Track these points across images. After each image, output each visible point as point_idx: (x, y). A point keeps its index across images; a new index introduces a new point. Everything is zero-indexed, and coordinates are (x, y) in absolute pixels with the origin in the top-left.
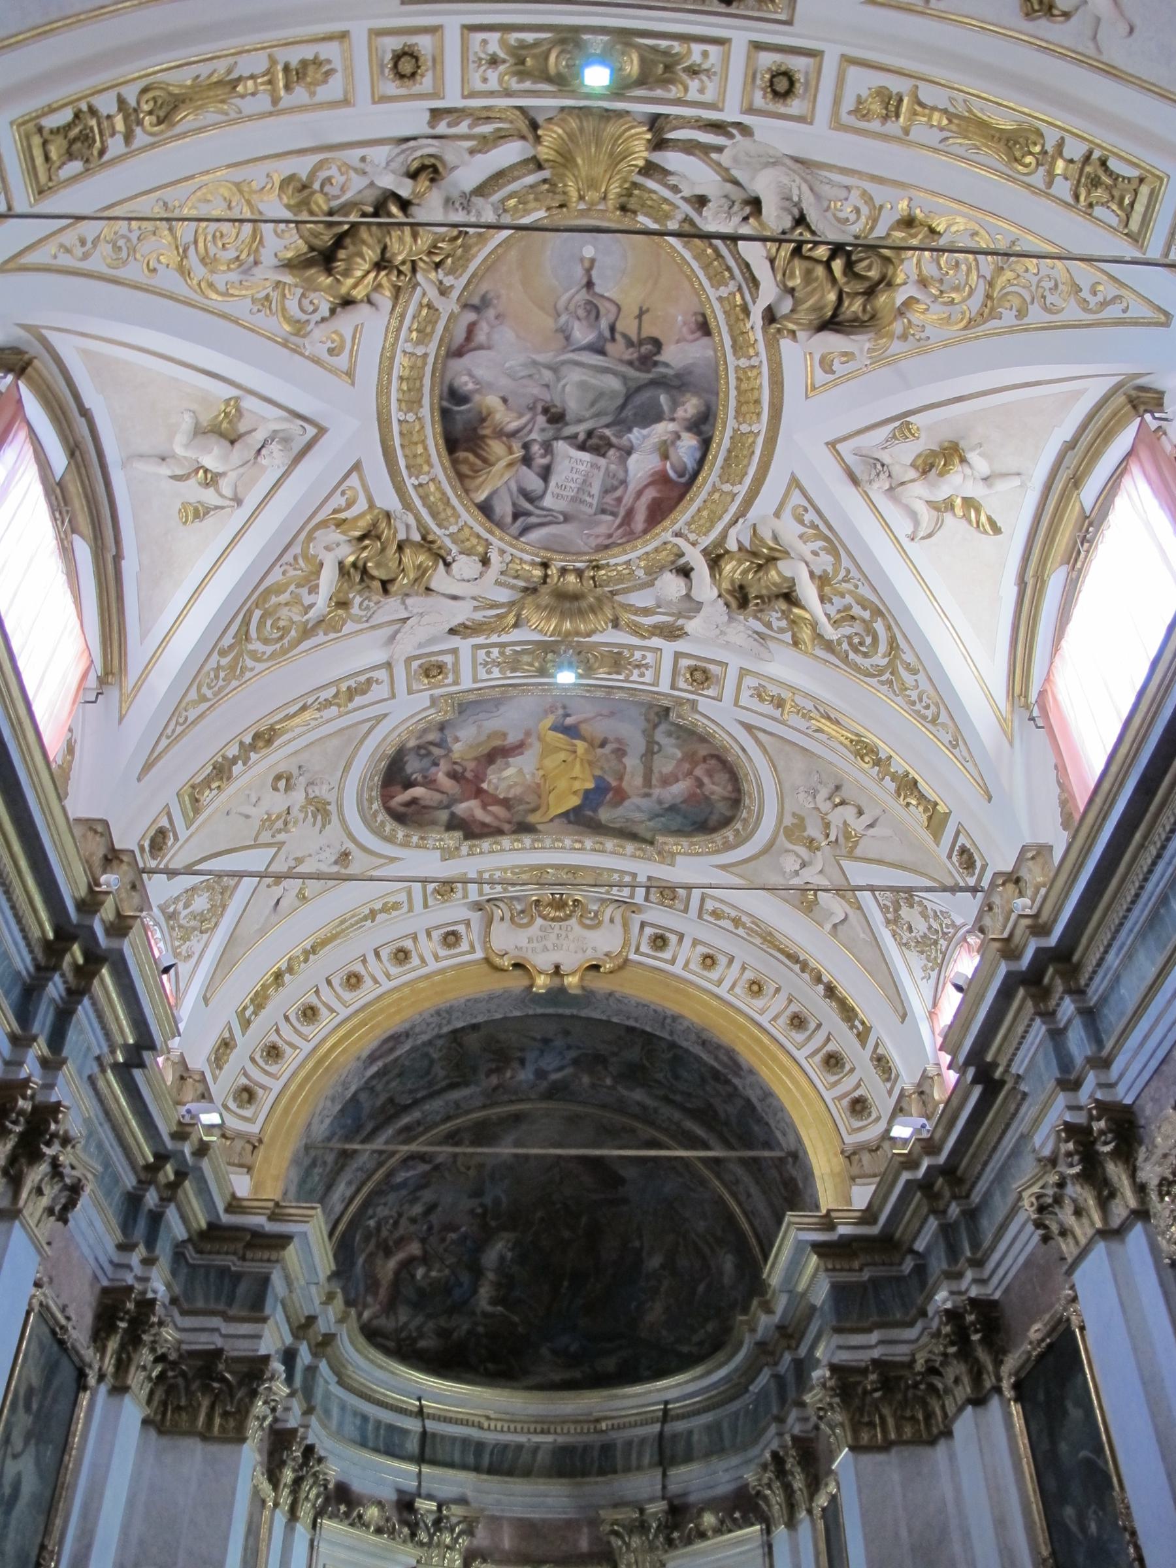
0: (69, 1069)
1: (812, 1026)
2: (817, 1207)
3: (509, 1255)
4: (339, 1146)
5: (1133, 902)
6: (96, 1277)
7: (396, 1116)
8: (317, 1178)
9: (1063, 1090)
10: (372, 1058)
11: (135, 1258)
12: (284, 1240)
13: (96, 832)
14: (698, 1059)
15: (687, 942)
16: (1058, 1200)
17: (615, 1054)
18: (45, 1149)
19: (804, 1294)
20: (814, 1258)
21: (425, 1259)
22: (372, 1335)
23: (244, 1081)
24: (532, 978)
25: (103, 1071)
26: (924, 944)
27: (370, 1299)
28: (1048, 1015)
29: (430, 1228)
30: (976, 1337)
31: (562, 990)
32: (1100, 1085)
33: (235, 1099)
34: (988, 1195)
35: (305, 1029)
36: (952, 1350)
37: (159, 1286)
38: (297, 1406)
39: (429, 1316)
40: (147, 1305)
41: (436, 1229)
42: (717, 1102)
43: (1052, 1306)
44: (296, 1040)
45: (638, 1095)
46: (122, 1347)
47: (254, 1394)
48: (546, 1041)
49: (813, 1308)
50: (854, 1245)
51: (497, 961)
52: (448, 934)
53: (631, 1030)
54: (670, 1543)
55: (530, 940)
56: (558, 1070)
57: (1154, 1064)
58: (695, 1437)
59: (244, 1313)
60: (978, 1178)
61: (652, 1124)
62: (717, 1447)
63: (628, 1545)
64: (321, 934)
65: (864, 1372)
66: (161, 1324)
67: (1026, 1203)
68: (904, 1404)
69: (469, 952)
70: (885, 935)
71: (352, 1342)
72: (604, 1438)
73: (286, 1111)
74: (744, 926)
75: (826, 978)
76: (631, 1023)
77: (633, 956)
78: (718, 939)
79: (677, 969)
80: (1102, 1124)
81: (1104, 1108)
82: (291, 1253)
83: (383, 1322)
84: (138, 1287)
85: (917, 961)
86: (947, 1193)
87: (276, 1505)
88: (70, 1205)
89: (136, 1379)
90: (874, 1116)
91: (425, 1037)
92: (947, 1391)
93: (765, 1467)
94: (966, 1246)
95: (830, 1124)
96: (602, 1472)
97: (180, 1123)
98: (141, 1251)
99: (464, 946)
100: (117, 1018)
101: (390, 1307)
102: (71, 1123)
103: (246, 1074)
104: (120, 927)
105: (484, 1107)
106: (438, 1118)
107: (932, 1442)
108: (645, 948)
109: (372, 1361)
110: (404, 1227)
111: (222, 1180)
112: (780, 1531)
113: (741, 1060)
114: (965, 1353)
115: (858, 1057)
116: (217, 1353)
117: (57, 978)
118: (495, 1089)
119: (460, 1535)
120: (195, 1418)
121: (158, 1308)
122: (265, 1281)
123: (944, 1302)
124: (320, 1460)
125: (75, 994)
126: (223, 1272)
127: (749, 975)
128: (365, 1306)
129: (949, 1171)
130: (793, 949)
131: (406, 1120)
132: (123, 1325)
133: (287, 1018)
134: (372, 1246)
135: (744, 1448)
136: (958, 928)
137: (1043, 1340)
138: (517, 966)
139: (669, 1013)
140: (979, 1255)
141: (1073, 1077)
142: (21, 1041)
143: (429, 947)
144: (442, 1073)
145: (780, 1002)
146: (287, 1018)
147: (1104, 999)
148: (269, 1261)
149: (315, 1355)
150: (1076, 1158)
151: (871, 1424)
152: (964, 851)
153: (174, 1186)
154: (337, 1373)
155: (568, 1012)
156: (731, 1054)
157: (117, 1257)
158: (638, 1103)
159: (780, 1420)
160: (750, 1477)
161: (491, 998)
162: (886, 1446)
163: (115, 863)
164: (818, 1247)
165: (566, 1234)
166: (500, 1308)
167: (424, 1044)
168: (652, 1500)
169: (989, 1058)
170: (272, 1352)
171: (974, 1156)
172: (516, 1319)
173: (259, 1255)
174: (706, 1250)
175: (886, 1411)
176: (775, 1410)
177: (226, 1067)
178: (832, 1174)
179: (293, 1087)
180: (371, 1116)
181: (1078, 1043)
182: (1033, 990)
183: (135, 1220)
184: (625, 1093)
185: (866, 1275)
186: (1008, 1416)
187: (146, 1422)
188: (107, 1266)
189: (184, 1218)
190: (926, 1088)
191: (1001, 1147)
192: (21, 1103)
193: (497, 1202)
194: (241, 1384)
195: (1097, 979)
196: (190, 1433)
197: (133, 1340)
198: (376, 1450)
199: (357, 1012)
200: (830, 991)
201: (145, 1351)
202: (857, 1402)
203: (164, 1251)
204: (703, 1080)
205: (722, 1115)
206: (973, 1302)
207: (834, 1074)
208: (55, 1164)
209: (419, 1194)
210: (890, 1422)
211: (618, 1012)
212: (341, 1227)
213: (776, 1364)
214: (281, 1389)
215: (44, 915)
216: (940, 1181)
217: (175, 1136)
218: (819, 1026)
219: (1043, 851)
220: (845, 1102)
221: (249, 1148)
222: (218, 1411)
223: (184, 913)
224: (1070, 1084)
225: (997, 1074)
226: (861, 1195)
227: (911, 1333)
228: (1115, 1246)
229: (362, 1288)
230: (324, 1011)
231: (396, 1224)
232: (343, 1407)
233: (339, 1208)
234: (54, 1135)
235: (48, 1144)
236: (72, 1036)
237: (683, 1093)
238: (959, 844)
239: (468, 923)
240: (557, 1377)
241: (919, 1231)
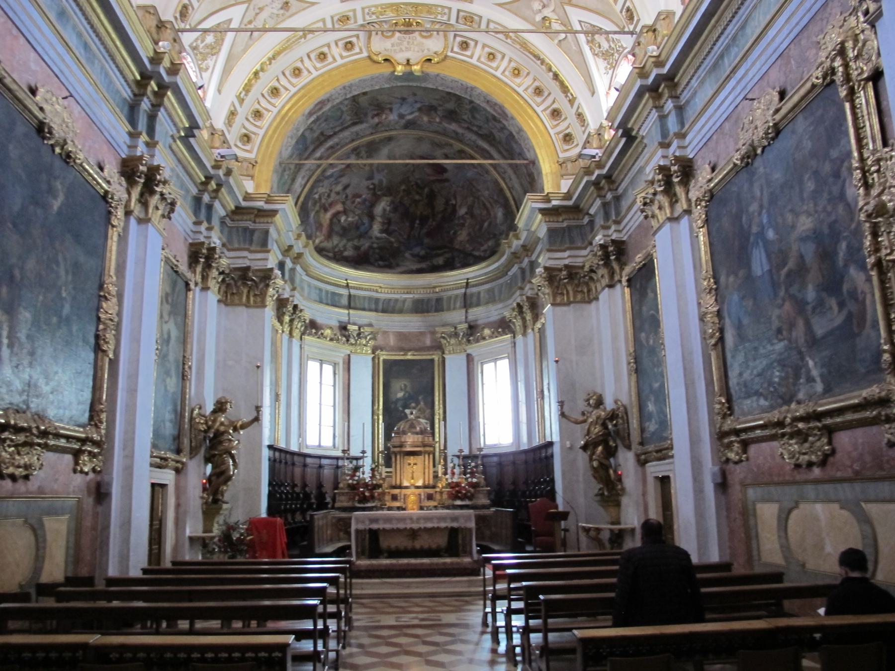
0: (160, 147)
1: (546, 94)
2: (542, 190)
3: (388, 208)
4: (297, 162)
5: (707, 55)
6: (186, 239)
7: (325, 140)
8: (286, 177)
9: (662, 147)
10: (311, 114)
11: (203, 228)
12: (274, 212)
13: (150, 13)
14: (485, 110)
15: (479, 46)
16: (652, 201)
17: (440, 106)
18: (157, 189)
19: (534, 232)
20: (540, 216)
21: (345, 212)
22: (320, 251)
23: (244, 131)
24: (394, 67)
25: (175, 141)
26: (606, 55)
27: (318, 234)
28: (659, 108)
29: (347, 197)
30: (613, 258)
31: (411, 73)
32: (679, 147)
34: (626, 190)
35: (273, 101)
36: (601, 263)
37: (216, 240)
38: (288, 288)
39: (348, 240)
40: (212, 250)
41: (350, 197)
42: (495, 131)
43: (648, 246)
44: (270, 107)
45: (453, 127)
46: (203, 270)
47: (267, 286)
48: (404, 99)
49: (539, 238)
50: (560, 210)
51: (375, 58)
52: (347, 43)
53: (449, 93)
54: (469, 341)
55: (393, 45)
56: (409, 112)
57: (705, 140)
58: (482, 295)
59: (259, 249)
60: (622, 181)
61: (461, 141)
62: (492, 298)
63: (449, 342)
64: (277, 48)
65: (560, 270)
66: (220, 257)
67: (638, 200)
68: (578, 285)
69: (360, 53)
70: (586, 49)
71: (312, 256)
73: (268, 146)
74: (511, 38)
75: (554, 69)
76: (449, 90)
77: (450, 54)
78: (496, 44)
79: (474, 61)
80: (676, 168)
81: (678, 160)
82: (278, 218)
84: (207, 242)
85: (602, 64)
86: (606, 187)
87: (283, 332)
88: (172, 210)
89: (213, 284)
90: (575, 143)
91: (338, 101)
92: (598, 280)
93: (513, 309)
94: (613, 213)
95: (552, 147)
96: (437, 311)
97: (216, 161)
98: (205, 225)
99: (357, 50)
100: (178, 115)
101: (329, 236)
102: (165, 174)
103: (244, 127)
104: (175, 69)
105: (372, 134)
107: (590, 302)
108: (456, 49)
109: (322, 264)
111: (240, 186)
112: (519, 337)
113: (507, 111)
114: (607, 264)
115: (569, 112)
116: (248, 269)
117: (145, 99)
118: (377, 125)
119: (370, 339)
120: (241, 298)
121: (218, 251)
122: (267, 232)
123: (600, 240)
124: (301, 311)
125: (156, 106)
126: (246, 229)
127: (513, 65)
128: (316, 237)
129: (608, 177)
130: (537, 52)
131: (330, 143)
132: (202, 260)
133: (263, 95)
134: (317, 208)
136: (625, 49)
138: (386, 60)
139: (469, 85)
140: (619, 219)
141: (667, 141)
142: (134, 135)
143: (336, 51)
144: (348, 118)
145: (528, 81)
146: (263, 95)
147: (688, 102)
149: (294, 263)
150: (662, 183)
151: (562, 294)
152: (628, 10)
153: (217, 191)
154: (305, 271)
155: (415, 84)
156: (501, 108)
157: (195, 228)
158: (454, 131)
159: (522, 289)
160: (507, 314)
161: (372, 79)
162: (569, 303)
163: (163, 29)
164: (543, 211)
165: (417, 197)
166: (384, 235)
167: (338, 104)
168: (460, 323)
169: (629, 126)
170: (274, 266)
171: (621, 171)
172: (393, 240)
173: (262, 220)
174: (488, 205)
175: (570, 288)
176: (520, 284)
177: (234, 125)
178: (552, 173)
179: (270, 132)
180: (312, 143)
181: (672, 124)
182: (653, 94)
183: (200, 209)
184: (446, 125)
185: (565, 224)
186: (623, 294)
187: (219, 301)
188: (191, 234)
189: (223, 206)
190: (602, 132)
191: (632, 170)
192: (141, 168)
193: (381, 181)
194: (261, 281)
195: (685, 92)
196: (239, 305)
197: (208, 266)
198: (327, 304)
200: (556, 76)
201: (214, 271)
202: (556, 284)
203: (216, 222)
204: (488, 120)
205: (497, 137)
206: (613, 241)
208: (162, 194)
209: (340, 180)
210: (571, 293)
211: (442, 85)
212: (301, 199)
213: (521, 263)
214: (280, 282)
215: (133, 68)
216: (603, 182)
217: (214, 167)
218: (550, 94)
219: (669, 15)
220: (561, 136)
221: (251, 166)
222: (252, 294)
223: (201, 46)
224: (665, 145)
225: (634, 133)
226: (565, 185)
227: (584, 252)
228: (675, 225)
229: (314, 230)
230: (282, 90)
232: (309, 285)
233: (299, 190)
234: (159, 181)
235: (157, 185)
236: (158, 128)
237: (477, 126)
238: (626, 6)
239: (358, 37)
240: (415, 266)
241: (592, 205)
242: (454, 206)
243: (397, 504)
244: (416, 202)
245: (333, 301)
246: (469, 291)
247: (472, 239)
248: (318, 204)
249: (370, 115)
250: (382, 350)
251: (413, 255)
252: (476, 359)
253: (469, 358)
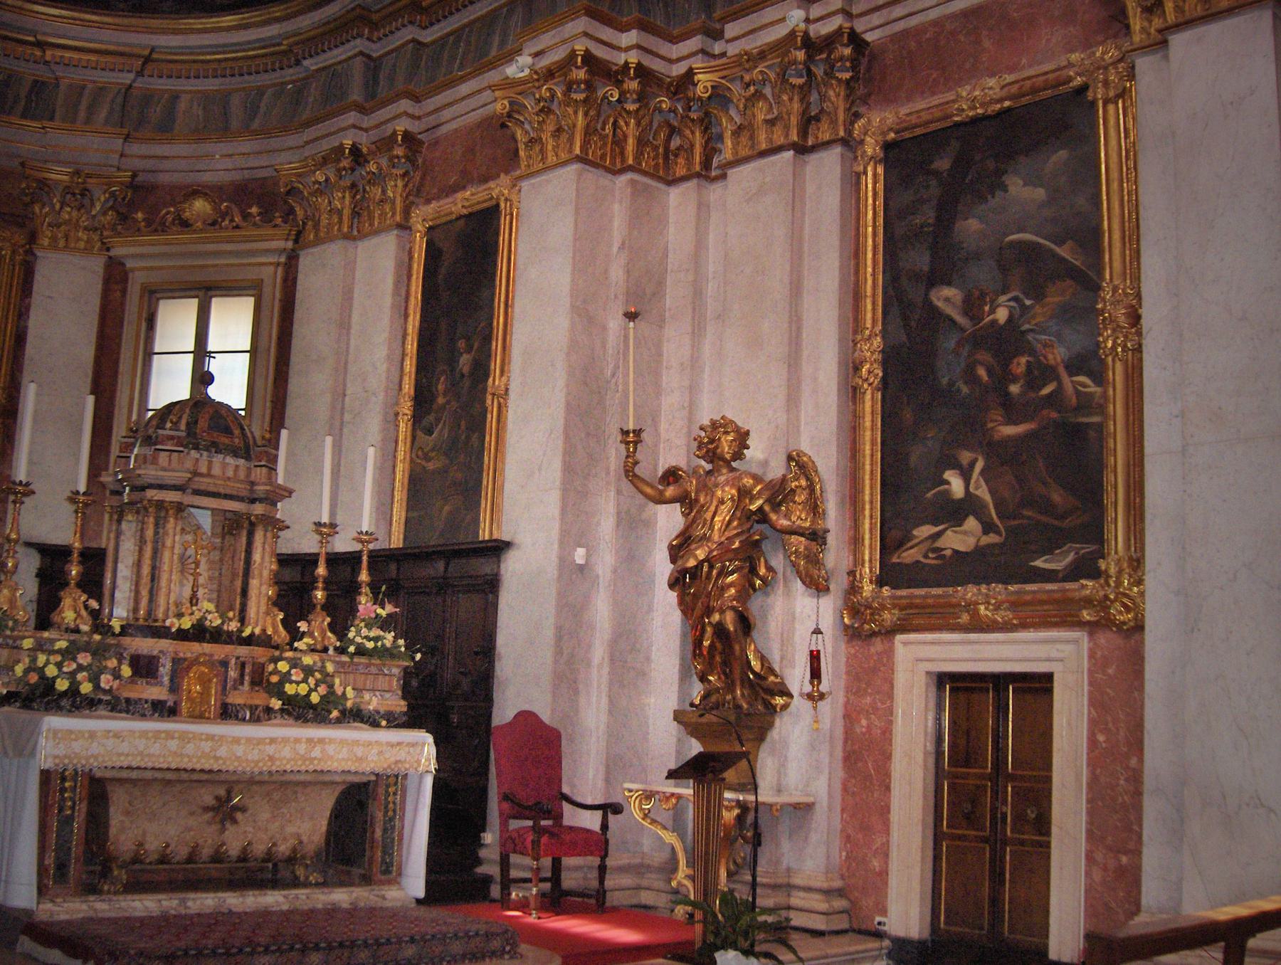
58: (182, 105)
135: (266, 132)
137: (1001, 100)
253: (115, 276)
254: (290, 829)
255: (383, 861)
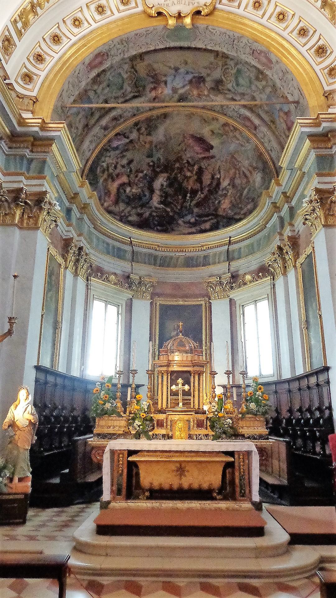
1: (311, 32)
3: (165, 184)
17: (208, 75)
21: (129, 184)
23: (25, 70)
29: (131, 171)
33: (21, 78)
39: (133, 208)
47: (41, 209)
48: (177, 69)
51: (149, 11)
54: (232, 288)
58: (242, 250)
62: (251, 250)
72: (205, 253)
77: (218, 6)
79: (241, 11)
82: (54, 147)
83: (112, 208)
101: (116, 202)
106: (129, 115)
110: (119, 170)
116: (21, 190)
122: (44, 162)
126: (22, 157)
127: (278, 10)
133: (44, 40)
138: (160, 14)
144: (129, 89)
146: (44, 40)
148: (44, 152)
149: (81, 213)
164: (311, 136)
165: (188, 174)
166: (162, 205)
172: (169, 210)
173: (39, 149)
174: (248, 173)
193: (159, 159)
194: (35, 205)
196: (13, 225)
199: (80, 40)
207: (321, 57)
212: (90, 162)
213: (280, 211)
218: (315, 32)
221: (31, 102)
222: (26, 216)
231: (115, 167)
232: (98, 239)
240: (186, 232)
242: (219, 179)
243: (163, 431)
244: (188, 178)
245: (119, 254)
246: (232, 247)
247: (233, 206)
248: (106, 173)
249: (148, 89)
250: (159, 297)
251: (185, 223)
252: (238, 303)
253: (232, 302)
254: (206, 479)
255: (241, 492)
